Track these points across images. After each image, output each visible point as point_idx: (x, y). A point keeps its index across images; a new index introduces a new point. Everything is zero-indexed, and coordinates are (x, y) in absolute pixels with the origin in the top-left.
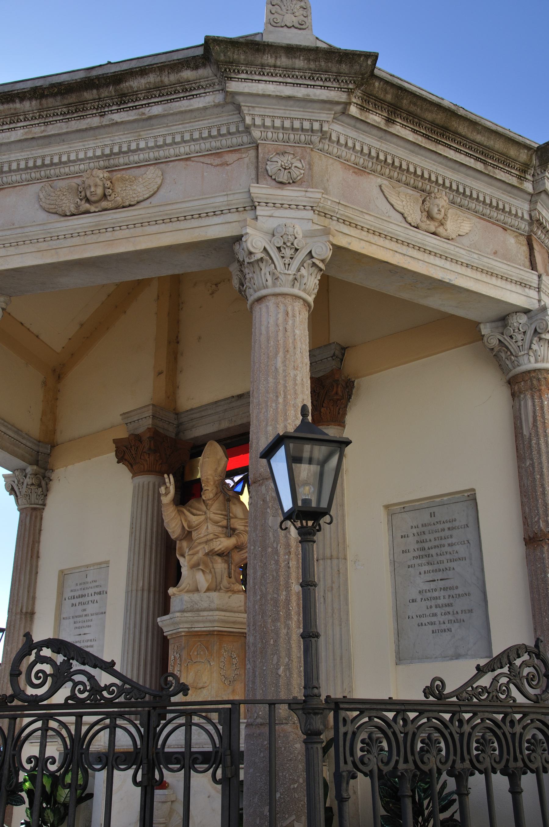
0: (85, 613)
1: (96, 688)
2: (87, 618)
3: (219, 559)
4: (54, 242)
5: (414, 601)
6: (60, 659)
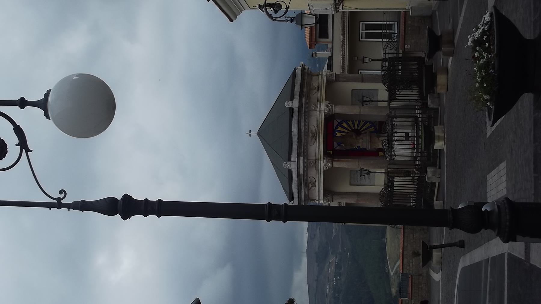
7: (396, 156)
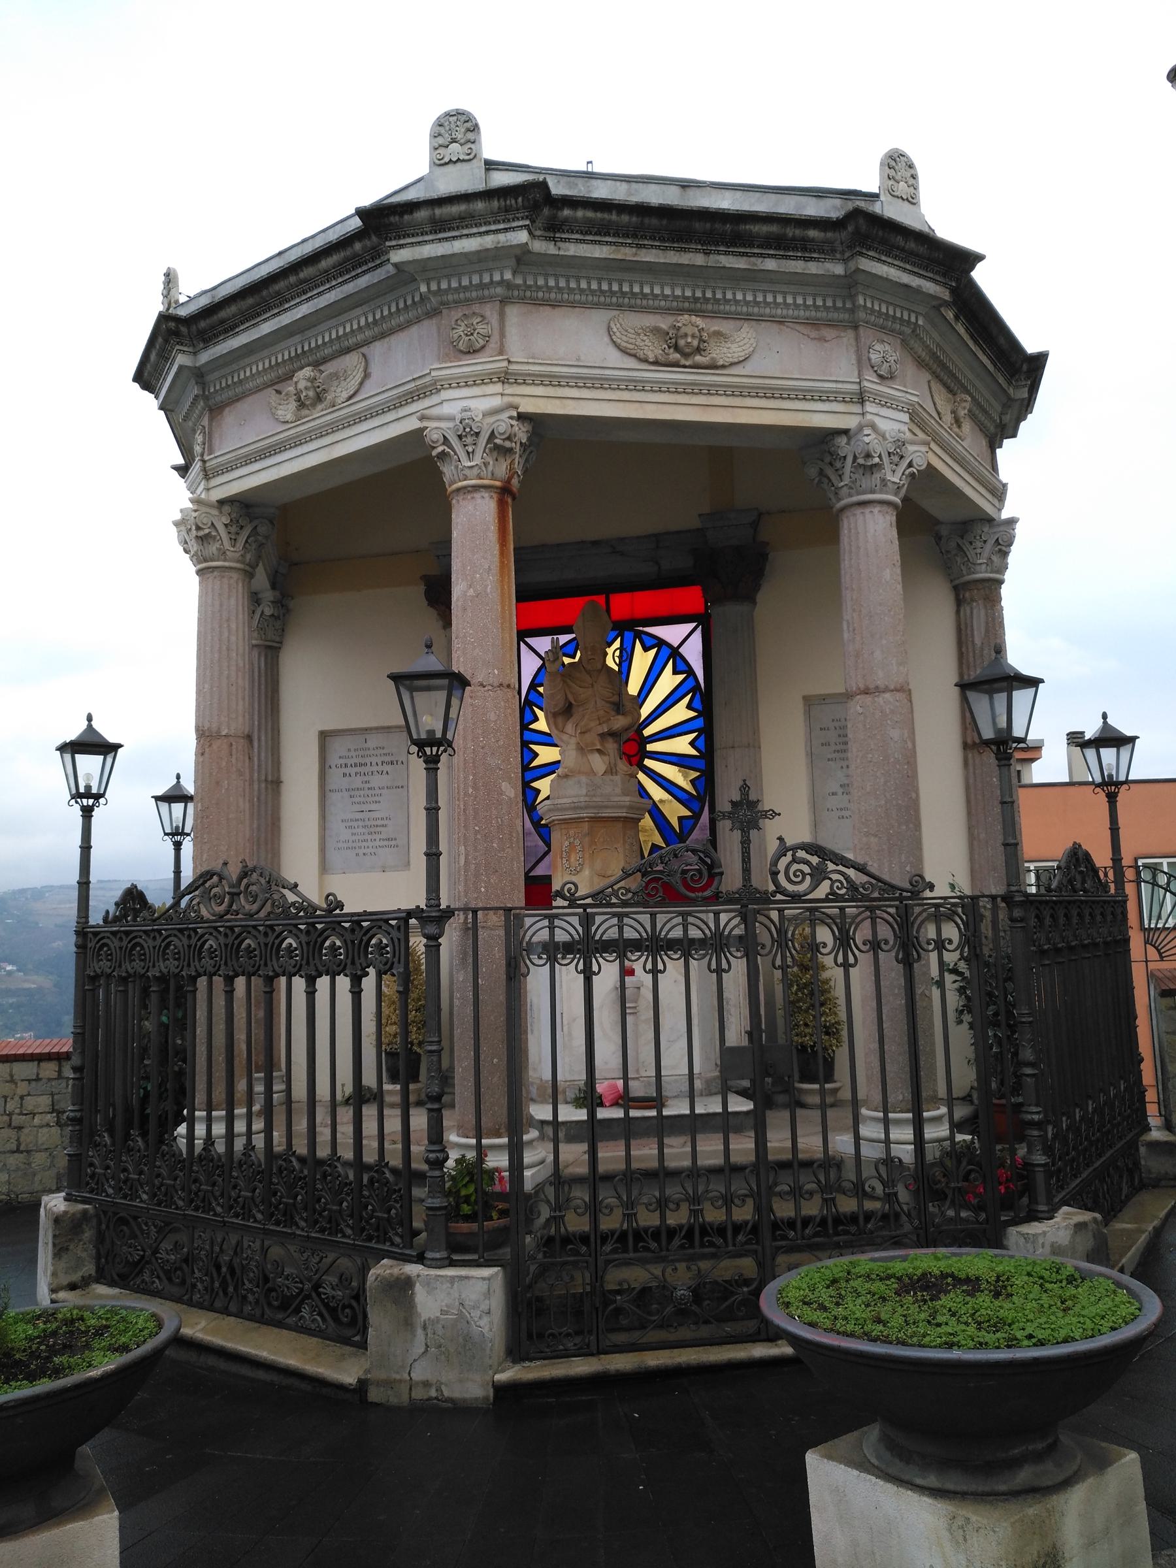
0: (367, 785)
1: (852, 886)
2: (373, 792)
3: (610, 740)
4: (639, 394)
5: (833, 794)
6: (815, 860)
7: (588, 976)
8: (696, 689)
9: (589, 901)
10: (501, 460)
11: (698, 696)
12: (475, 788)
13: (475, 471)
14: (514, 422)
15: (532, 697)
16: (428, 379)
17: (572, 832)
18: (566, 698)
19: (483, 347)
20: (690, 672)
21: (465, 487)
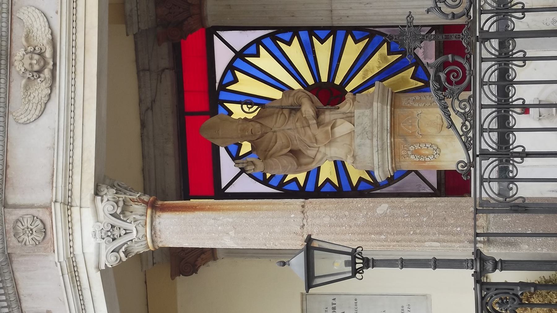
3: (322, 117)
7: (525, 155)
8: (273, 37)
9: (471, 152)
10: (131, 209)
11: (280, 36)
12: (380, 233)
13: (140, 228)
14: (105, 198)
15: (274, 182)
16: (64, 265)
17: (403, 153)
18: (285, 155)
19: (42, 221)
20: (258, 42)
21: (152, 236)
